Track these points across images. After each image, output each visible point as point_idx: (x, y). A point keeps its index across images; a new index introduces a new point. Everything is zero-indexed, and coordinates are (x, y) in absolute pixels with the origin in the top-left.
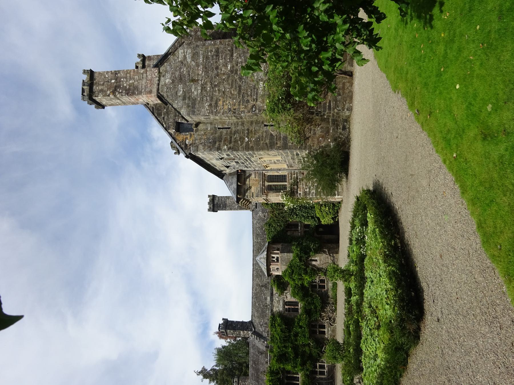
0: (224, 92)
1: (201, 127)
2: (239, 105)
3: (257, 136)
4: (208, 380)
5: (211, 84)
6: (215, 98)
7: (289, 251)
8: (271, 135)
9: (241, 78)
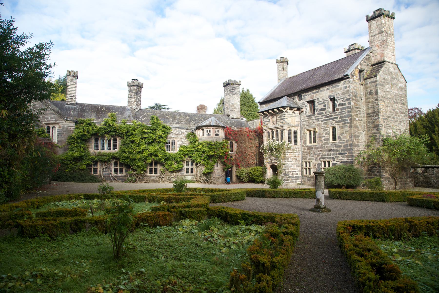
0: (387, 106)
2: (383, 116)
3: (359, 127)
5: (391, 98)
6: (384, 100)
8: (359, 136)
9: (393, 118)
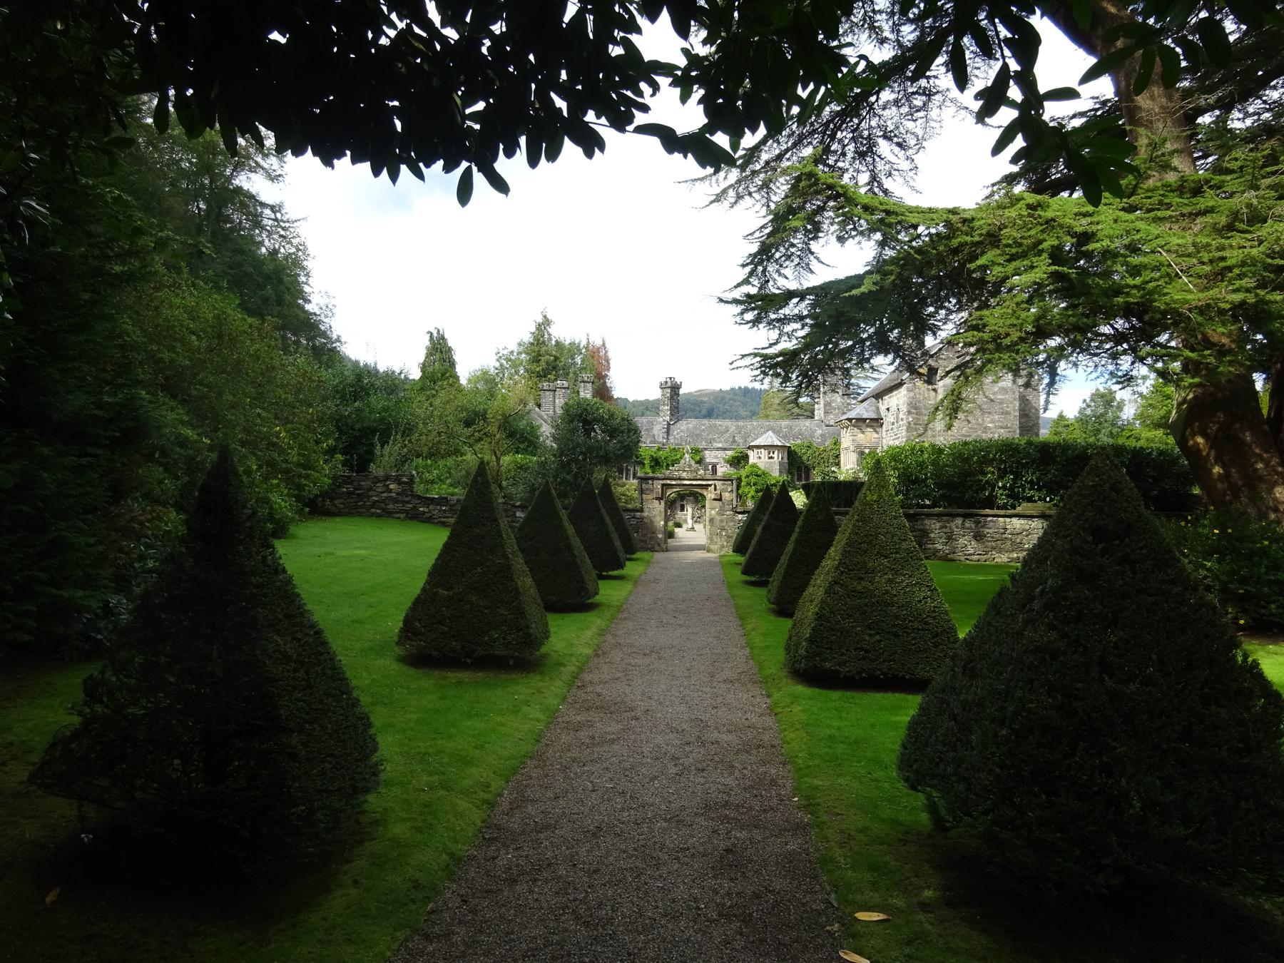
1: (933, 393)
4: (533, 330)
7: (781, 472)
